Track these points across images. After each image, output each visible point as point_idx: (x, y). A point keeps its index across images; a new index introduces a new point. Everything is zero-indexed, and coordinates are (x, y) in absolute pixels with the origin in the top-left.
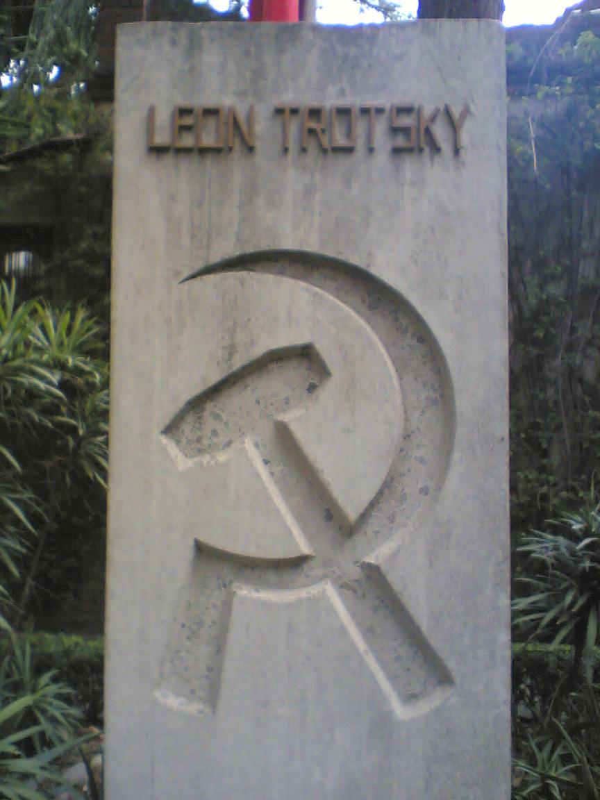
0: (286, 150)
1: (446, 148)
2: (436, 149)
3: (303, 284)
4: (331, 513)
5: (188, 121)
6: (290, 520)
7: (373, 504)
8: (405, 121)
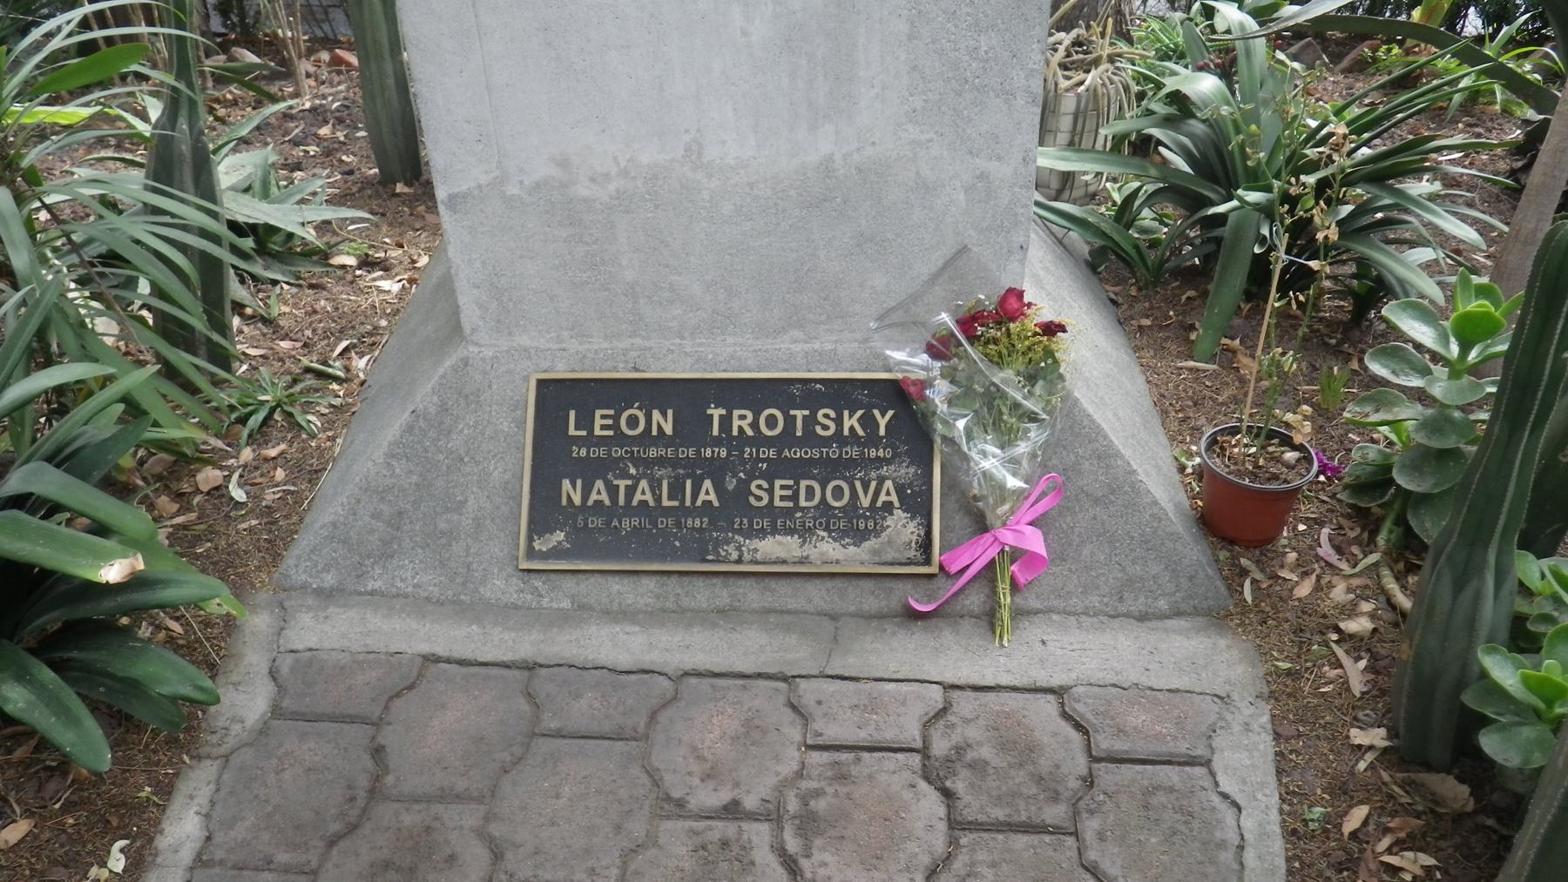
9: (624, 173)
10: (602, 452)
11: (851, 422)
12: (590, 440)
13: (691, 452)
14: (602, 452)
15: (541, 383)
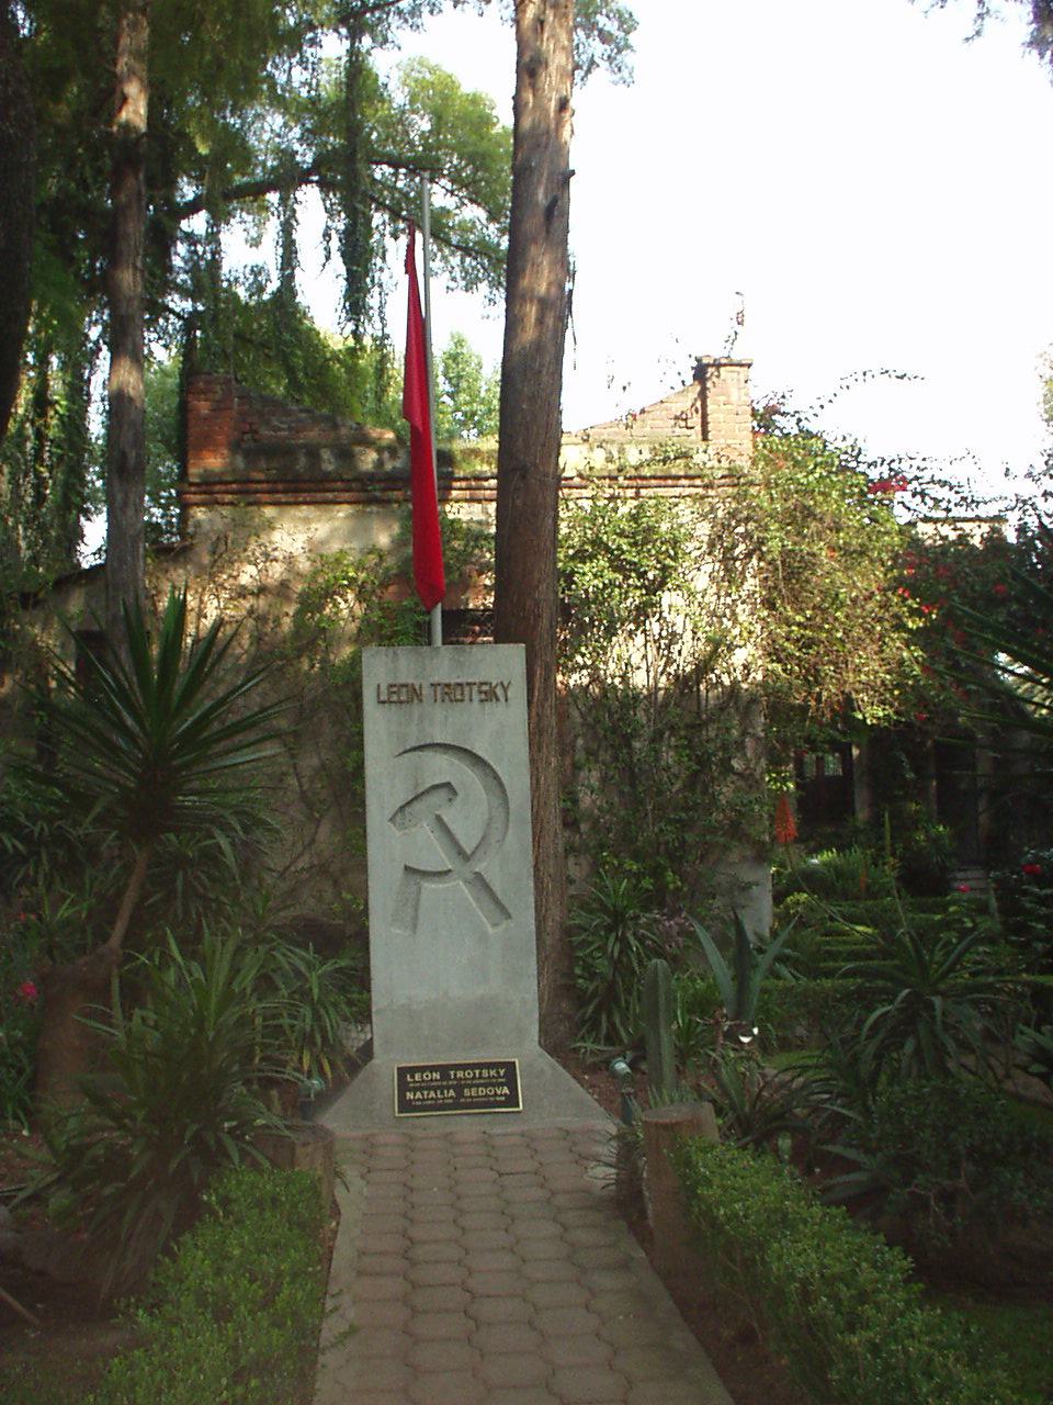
0: (436, 700)
1: (502, 699)
2: (498, 700)
3: (446, 757)
4: (461, 852)
5: (395, 689)
6: (443, 856)
7: (477, 848)
8: (485, 688)
9: (426, 1001)
10: (418, 1084)
11: (493, 1073)
12: (415, 1082)
13: (445, 1083)
14: (418, 1084)
15: (399, 1069)
